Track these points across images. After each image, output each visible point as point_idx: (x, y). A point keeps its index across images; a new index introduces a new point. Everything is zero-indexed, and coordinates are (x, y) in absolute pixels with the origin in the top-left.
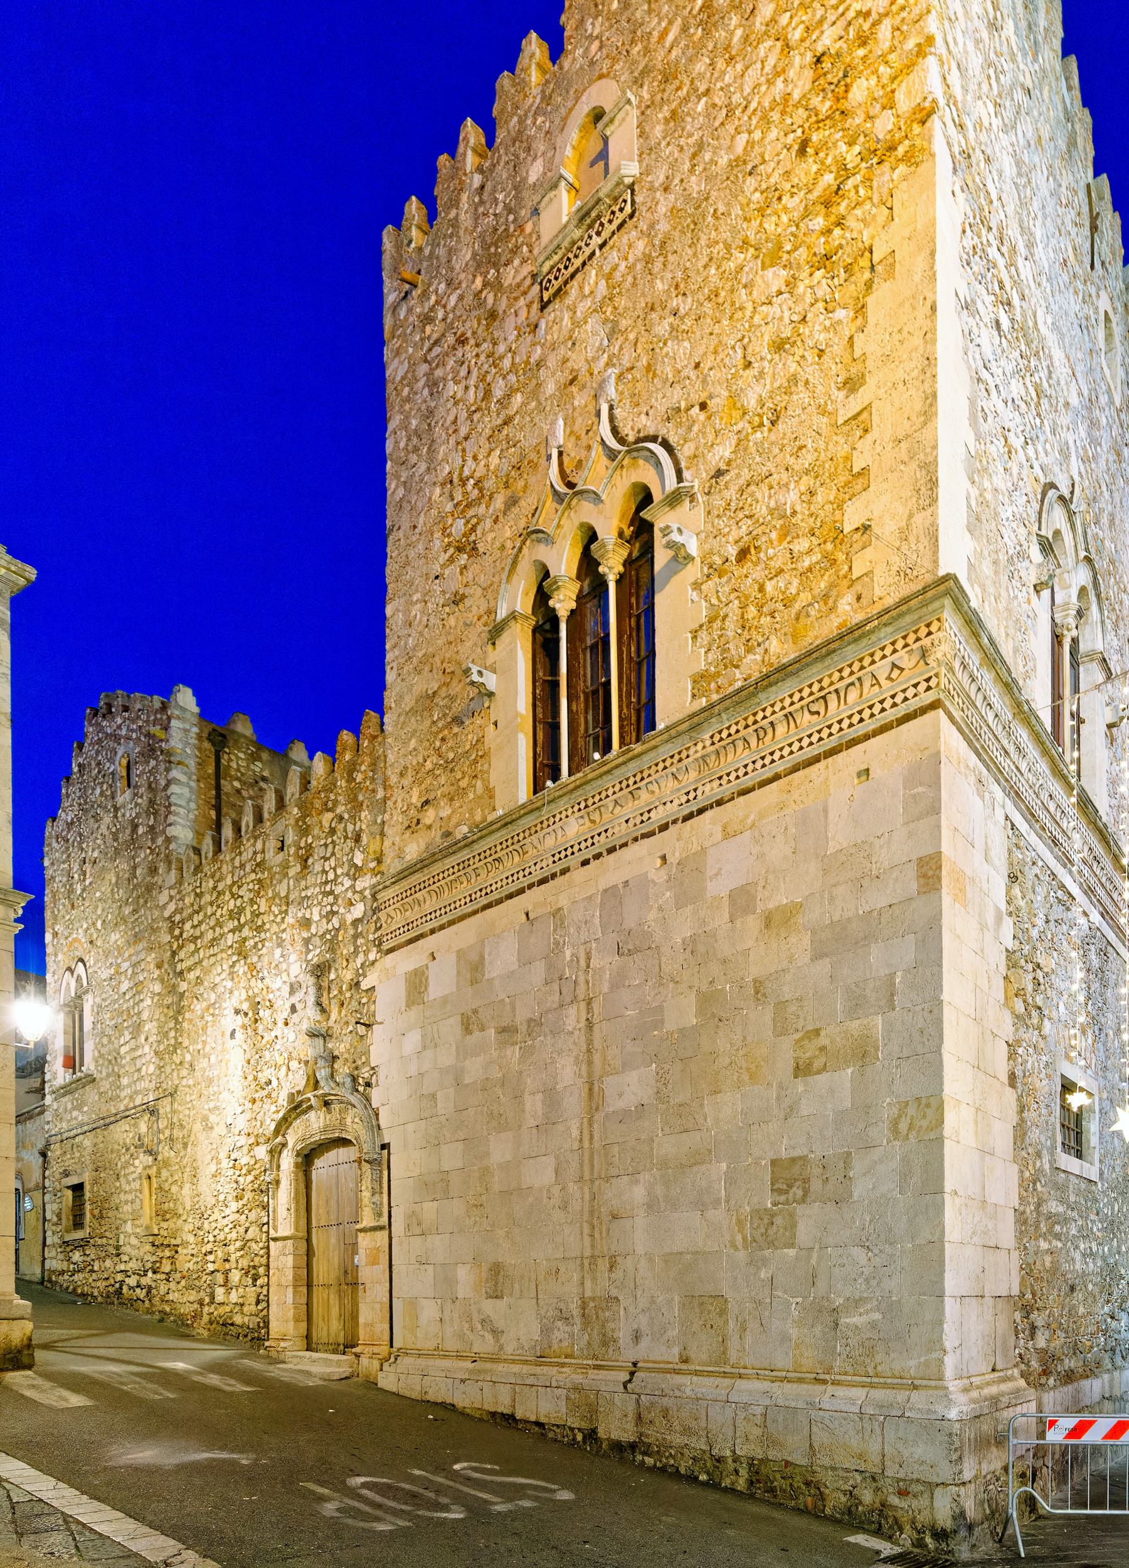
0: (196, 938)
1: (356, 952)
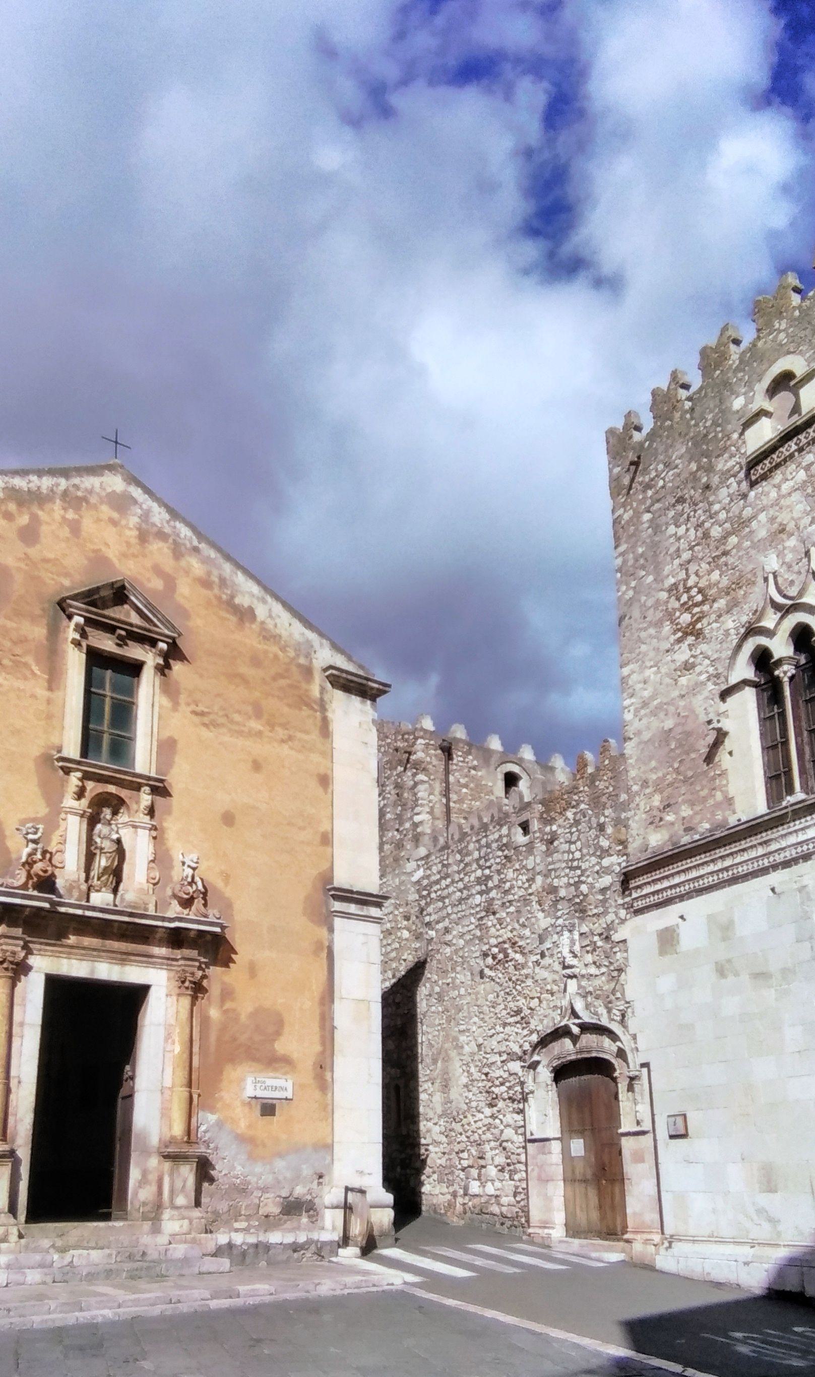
0: (444, 898)
1: (605, 913)
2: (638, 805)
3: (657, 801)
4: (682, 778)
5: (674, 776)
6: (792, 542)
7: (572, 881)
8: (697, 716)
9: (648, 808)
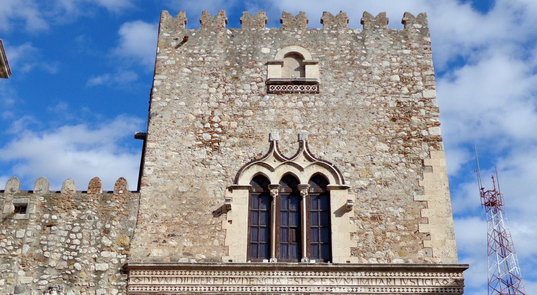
3: (163, 229)
5: (182, 220)
6: (290, 132)
7: (66, 258)
8: (207, 193)
9: (155, 232)
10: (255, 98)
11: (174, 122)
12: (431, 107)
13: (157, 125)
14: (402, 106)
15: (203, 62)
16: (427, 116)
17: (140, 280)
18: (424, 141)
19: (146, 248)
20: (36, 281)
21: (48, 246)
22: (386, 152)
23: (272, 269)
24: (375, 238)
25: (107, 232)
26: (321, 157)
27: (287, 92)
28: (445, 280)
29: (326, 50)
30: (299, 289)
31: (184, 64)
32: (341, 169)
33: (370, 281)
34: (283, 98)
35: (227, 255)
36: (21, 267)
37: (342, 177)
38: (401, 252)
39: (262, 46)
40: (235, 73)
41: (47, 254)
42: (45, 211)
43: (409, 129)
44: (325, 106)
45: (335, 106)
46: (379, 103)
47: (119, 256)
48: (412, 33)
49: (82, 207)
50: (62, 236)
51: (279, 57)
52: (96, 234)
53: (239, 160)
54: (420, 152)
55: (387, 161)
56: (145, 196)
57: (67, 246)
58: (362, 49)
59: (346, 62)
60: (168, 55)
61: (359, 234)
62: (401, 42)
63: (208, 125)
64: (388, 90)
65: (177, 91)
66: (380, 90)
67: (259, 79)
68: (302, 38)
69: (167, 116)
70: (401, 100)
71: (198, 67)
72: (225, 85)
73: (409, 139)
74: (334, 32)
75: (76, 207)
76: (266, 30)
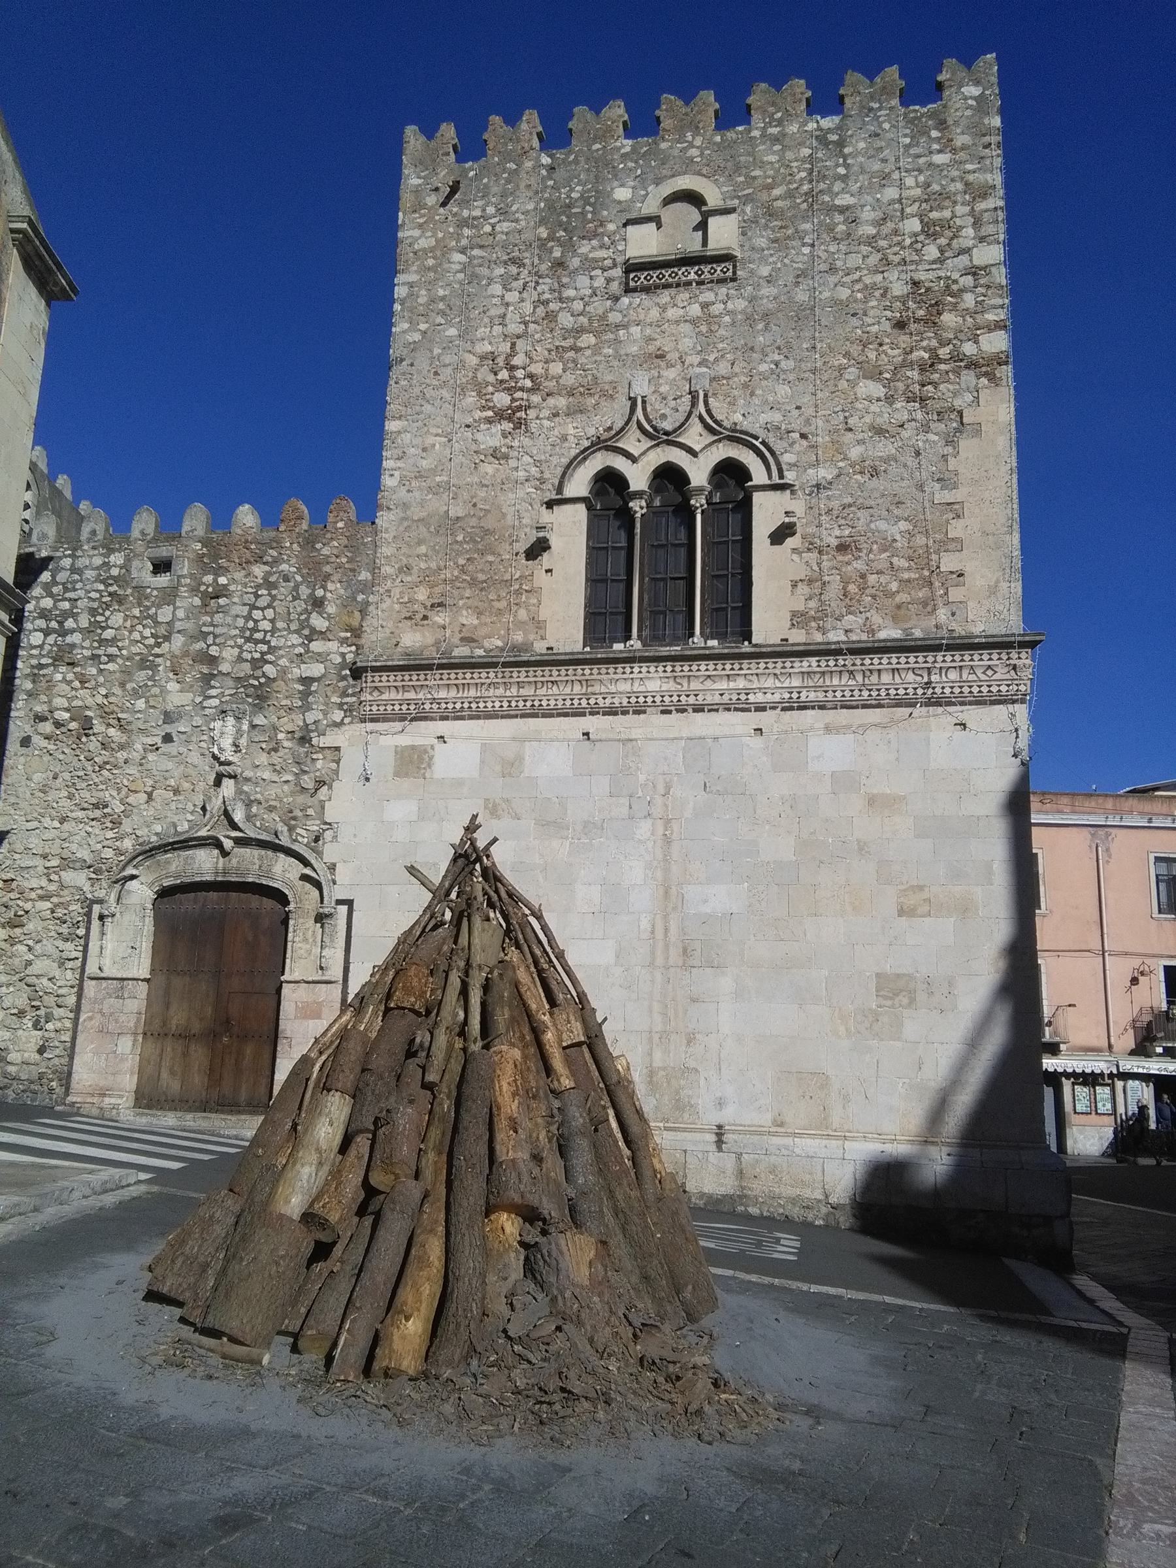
2: (389, 591)
3: (422, 594)
4: (468, 578)
5: (456, 573)
6: (671, 374)
8: (504, 515)
9: (406, 599)
10: (598, 306)
11: (436, 373)
12: (988, 287)
13: (403, 383)
14: (923, 290)
15: (492, 234)
16: (979, 308)
17: (382, 693)
18: (967, 367)
19: (391, 631)
20: (198, 699)
21: (215, 637)
22: (879, 400)
23: (630, 659)
24: (844, 588)
25: (318, 604)
26: (736, 424)
27: (667, 286)
28: (989, 667)
29: (755, 178)
30: (683, 698)
31: (454, 243)
32: (778, 446)
33: (827, 677)
34: (657, 300)
35: (543, 638)
36: (171, 675)
37: (778, 464)
38: (897, 614)
39: (616, 183)
40: (557, 253)
41: (214, 651)
42: (206, 569)
43: (934, 343)
44: (749, 310)
45: (771, 306)
46: (868, 290)
47: (342, 650)
48: (956, 110)
49: (270, 559)
50: (237, 616)
51: (651, 206)
52: (299, 609)
53: (566, 445)
54: (955, 394)
55: (879, 420)
56: (387, 531)
57: (248, 634)
58: (837, 165)
59: (798, 201)
60: (420, 226)
61: (810, 581)
62: (929, 136)
63: (504, 375)
64: (891, 257)
65: (441, 306)
66: (874, 259)
67: (608, 263)
68: (702, 155)
69: (422, 363)
70: (921, 276)
71: (482, 247)
72: (537, 283)
73: (932, 365)
74: (774, 131)
75: (259, 559)
76: (623, 146)
